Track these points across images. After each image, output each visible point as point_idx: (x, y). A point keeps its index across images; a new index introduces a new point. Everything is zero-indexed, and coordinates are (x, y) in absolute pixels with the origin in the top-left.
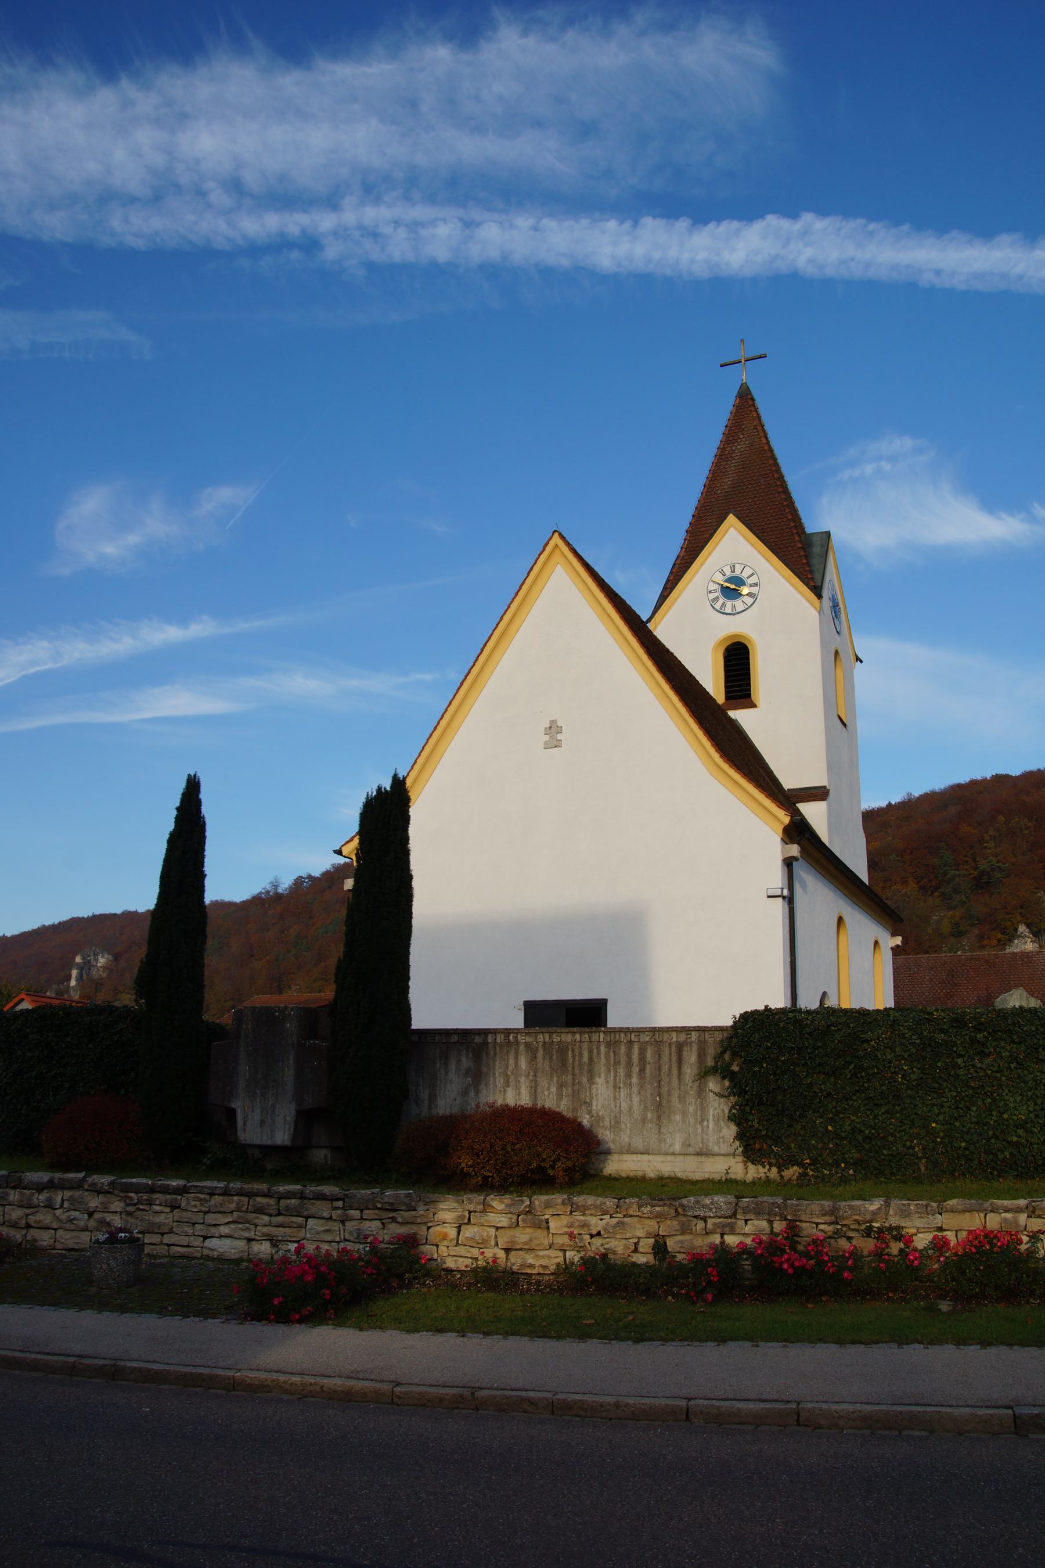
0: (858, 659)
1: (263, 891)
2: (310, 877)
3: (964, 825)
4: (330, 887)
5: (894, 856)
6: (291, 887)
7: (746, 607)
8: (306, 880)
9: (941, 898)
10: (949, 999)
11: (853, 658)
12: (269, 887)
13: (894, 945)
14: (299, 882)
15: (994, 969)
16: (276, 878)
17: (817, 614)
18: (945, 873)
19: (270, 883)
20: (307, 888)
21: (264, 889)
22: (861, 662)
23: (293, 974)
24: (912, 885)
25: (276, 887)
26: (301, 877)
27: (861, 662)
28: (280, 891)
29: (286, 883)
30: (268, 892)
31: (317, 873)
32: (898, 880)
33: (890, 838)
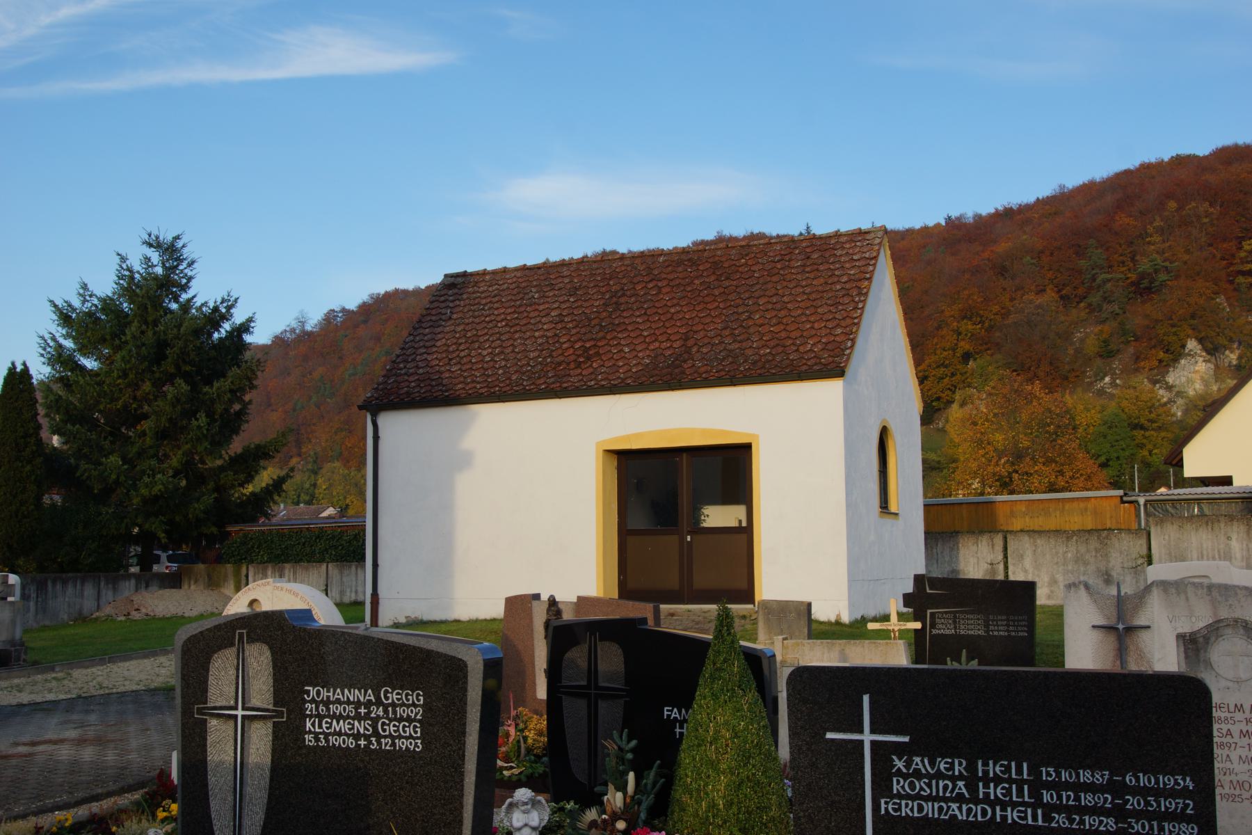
1: (288, 329)
2: (344, 310)
3: (1123, 215)
4: (365, 322)
5: (1028, 258)
6: (320, 323)
8: (340, 315)
9: (1087, 310)
10: (579, 365)
12: (294, 324)
14: (330, 317)
15: (727, 283)
16: (301, 312)
18: (1094, 278)
19: (295, 319)
20: (341, 322)
21: (288, 326)
23: (314, 424)
24: (1050, 296)
25: (303, 323)
26: (333, 310)
28: (308, 328)
29: (314, 319)
30: (293, 330)
31: (352, 305)
32: (1033, 287)
33: (1025, 237)
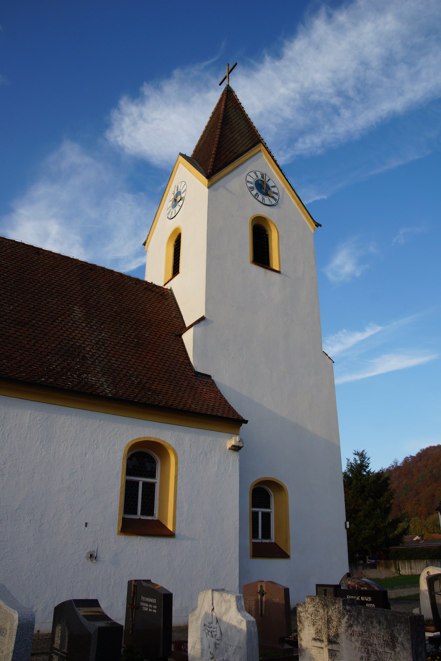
0: (318, 225)
1: (391, 466)
2: (411, 457)
4: (420, 460)
6: (403, 462)
7: (180, 208)
8: (410, 459)
11: (311, 227)
12: (393, 464)
13: (230, 446)
14: (406, 460)
16: (395, 459)
17: (207, 190)
19: (393, 462)
20: (411, 461)
21: (391, 465)
22: (321, 226)
23: (405, 502)
25: (396, 463)
26: (407, 457)
27: (321, 226)
28: (398, 465)
29: (400, 461)
30: (393, 466)
31: (414, 454)
